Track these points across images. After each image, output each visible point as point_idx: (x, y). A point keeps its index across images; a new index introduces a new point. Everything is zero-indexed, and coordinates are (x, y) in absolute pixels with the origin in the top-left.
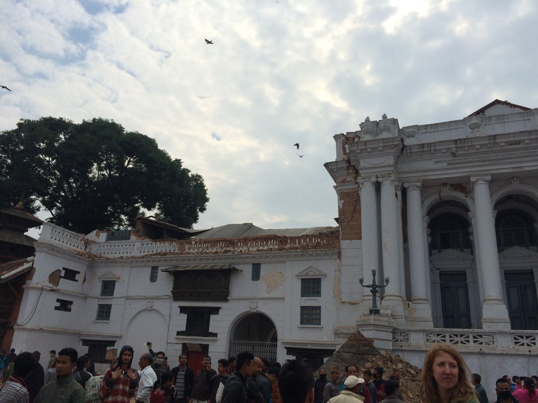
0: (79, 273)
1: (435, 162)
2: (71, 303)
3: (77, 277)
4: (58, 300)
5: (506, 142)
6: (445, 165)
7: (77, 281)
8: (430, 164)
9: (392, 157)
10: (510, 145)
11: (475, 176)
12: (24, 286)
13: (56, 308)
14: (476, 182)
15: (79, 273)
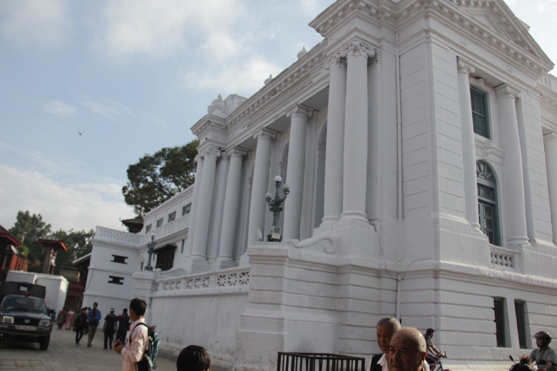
0: (127, 258)
1: (244, 126)
2: (123, 279)
3: (126, 261)
4: (110, 277)
5: (268, 94)
6: (246, 128)
7: (126, 263)
8: (241, 130)
9: (211, 132)
10: (273, 95)
11: (255, 134)
12: (89, 267)
13: (109, 282)
14: (257, 138)
15: (127, 258)
